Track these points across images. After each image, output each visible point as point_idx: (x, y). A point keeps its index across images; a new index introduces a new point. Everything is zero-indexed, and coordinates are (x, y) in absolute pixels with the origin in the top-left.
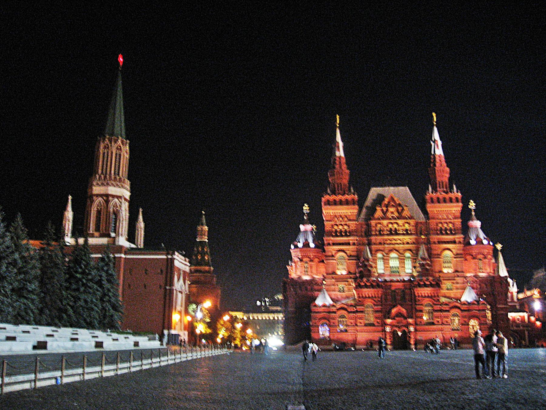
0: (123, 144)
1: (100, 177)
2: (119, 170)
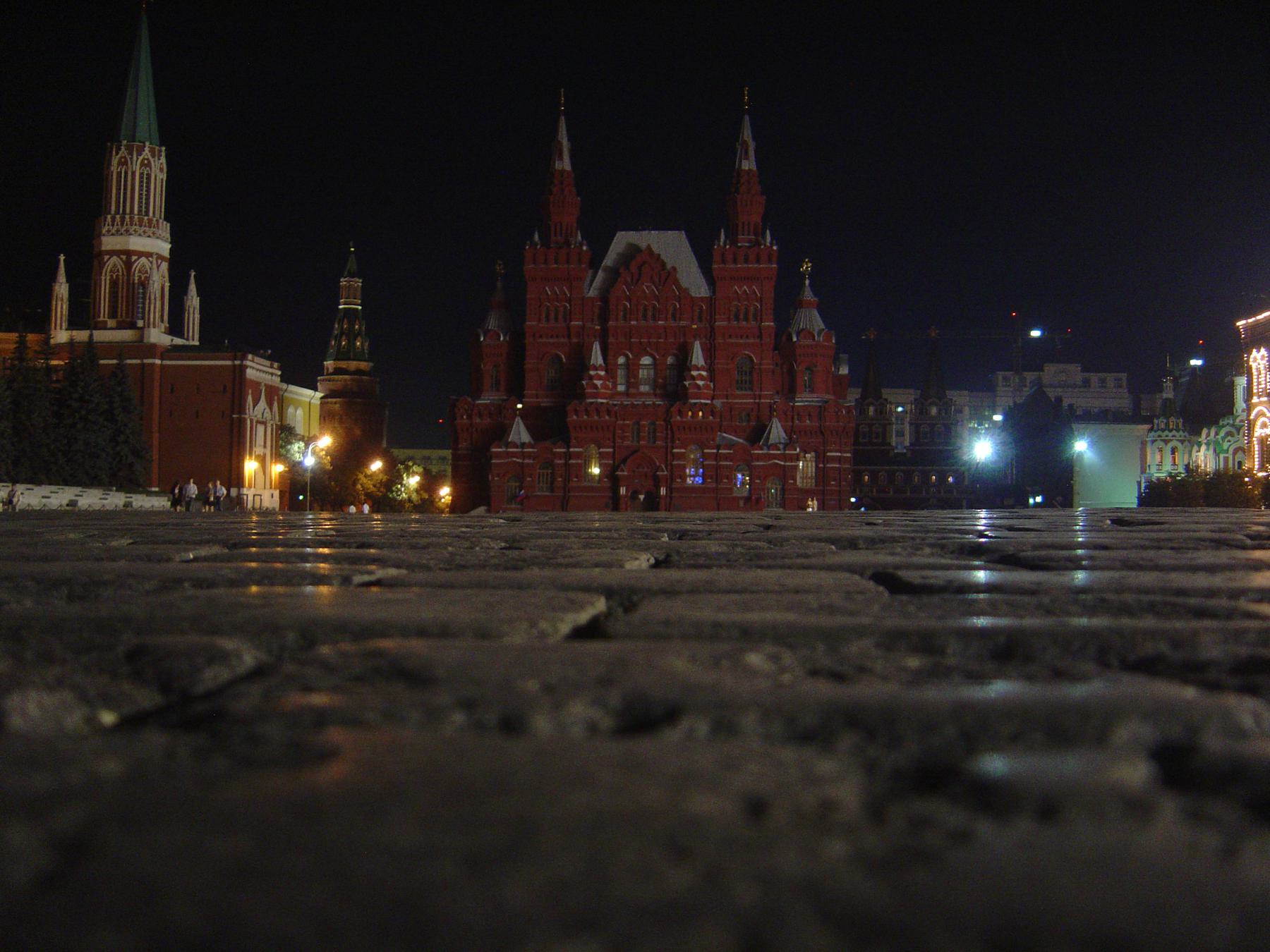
0: (153, 156)
1: (113, 219)
2: (147, 204)
